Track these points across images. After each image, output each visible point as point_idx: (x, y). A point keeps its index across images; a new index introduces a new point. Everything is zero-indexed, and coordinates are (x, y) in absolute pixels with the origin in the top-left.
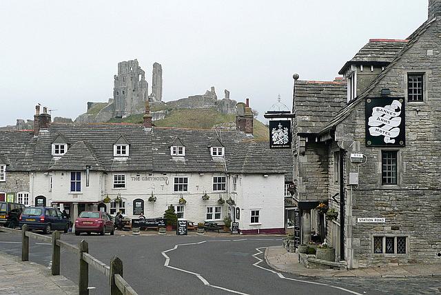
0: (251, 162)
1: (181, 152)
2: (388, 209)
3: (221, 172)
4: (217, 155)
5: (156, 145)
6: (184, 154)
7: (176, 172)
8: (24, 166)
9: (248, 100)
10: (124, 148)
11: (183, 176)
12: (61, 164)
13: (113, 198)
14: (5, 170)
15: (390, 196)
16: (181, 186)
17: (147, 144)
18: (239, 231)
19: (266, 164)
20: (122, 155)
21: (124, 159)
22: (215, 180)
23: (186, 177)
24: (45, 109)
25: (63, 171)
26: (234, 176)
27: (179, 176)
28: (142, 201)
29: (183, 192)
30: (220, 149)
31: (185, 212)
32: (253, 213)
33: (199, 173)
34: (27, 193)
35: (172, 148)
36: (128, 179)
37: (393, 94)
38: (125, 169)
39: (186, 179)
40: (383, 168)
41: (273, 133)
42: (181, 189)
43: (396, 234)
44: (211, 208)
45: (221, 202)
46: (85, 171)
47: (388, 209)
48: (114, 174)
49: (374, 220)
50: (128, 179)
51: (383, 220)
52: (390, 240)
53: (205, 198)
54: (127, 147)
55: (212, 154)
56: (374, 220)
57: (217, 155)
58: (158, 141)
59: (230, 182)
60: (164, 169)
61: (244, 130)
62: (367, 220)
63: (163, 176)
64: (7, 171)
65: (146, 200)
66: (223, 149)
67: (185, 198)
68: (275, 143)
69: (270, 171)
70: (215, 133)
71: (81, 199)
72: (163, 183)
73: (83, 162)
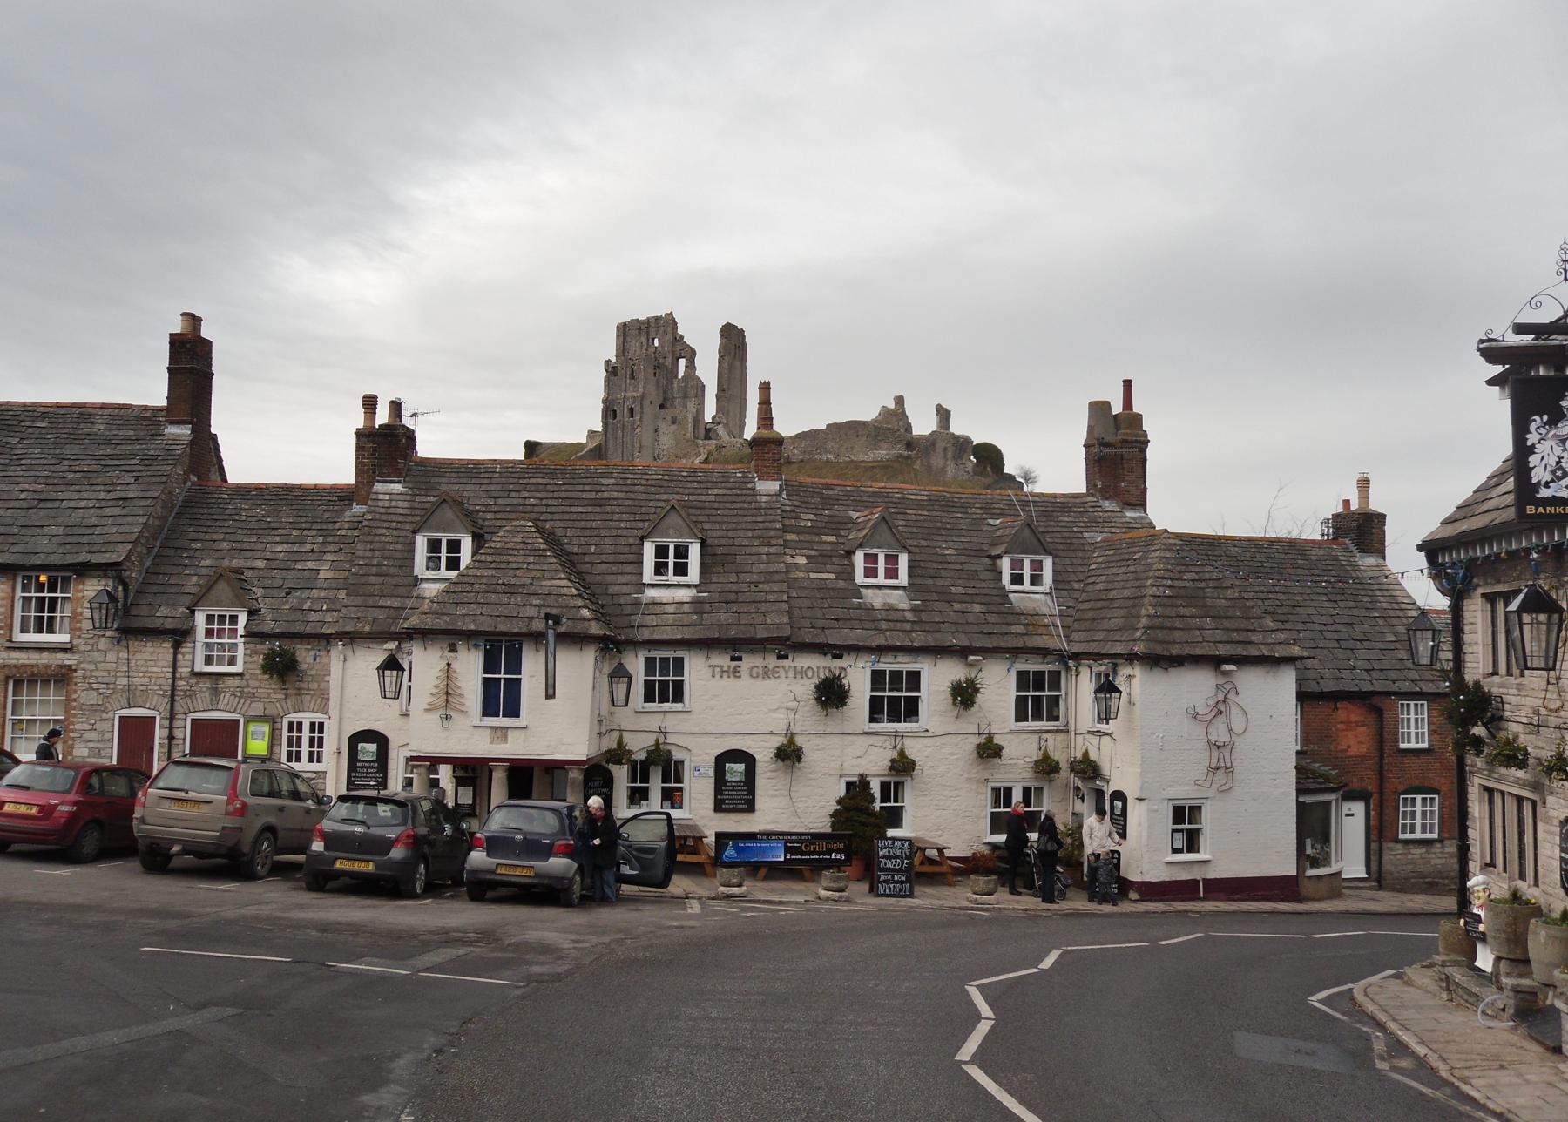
0: (1168, 612)
1: (892, 573)
3: (1043, 653)
4: (1027, 586)
5: (798, 546)
6: (903, 579)
7: (881, 650)
8: (313, 617)
9: (1128, 384)
10: (682, 552)
11: (904, 664)
13: (639, 745)
14: (241, 631)
16: (894, 701)
17: (766, 541)
18: (1125, 886)
19: (1227, 623)
20: (672, 578)
21: (685, 595)
23: (913, 667)
24: (396, 407)
27: (888, 664)
28: (747, 759)
29: (902, 726)
30: (1037, 566)
31: (910, 802)
32: (1179, 814)
34: (317, 717)
35: (859, 558)
36: (697, 671)
38: (687, 634)
39: (914, 679)
41: (1532, 438)
42: (895, 718)
44: (1008, 792)
45: (1046, 767)
46: (537, 638)
50: (697, 671)
53: (989, 751)
55: (1006, 579)
57: (1027, 586)
59: (1081, 690)
60: (835, 638)
64: (250, 634)
65: (763, 753)
66: (1048, 564)
67: (914, 750)
68: (1544, 493)
69: (1240, 650)
70: (1010, 504)
71: (518, 746)
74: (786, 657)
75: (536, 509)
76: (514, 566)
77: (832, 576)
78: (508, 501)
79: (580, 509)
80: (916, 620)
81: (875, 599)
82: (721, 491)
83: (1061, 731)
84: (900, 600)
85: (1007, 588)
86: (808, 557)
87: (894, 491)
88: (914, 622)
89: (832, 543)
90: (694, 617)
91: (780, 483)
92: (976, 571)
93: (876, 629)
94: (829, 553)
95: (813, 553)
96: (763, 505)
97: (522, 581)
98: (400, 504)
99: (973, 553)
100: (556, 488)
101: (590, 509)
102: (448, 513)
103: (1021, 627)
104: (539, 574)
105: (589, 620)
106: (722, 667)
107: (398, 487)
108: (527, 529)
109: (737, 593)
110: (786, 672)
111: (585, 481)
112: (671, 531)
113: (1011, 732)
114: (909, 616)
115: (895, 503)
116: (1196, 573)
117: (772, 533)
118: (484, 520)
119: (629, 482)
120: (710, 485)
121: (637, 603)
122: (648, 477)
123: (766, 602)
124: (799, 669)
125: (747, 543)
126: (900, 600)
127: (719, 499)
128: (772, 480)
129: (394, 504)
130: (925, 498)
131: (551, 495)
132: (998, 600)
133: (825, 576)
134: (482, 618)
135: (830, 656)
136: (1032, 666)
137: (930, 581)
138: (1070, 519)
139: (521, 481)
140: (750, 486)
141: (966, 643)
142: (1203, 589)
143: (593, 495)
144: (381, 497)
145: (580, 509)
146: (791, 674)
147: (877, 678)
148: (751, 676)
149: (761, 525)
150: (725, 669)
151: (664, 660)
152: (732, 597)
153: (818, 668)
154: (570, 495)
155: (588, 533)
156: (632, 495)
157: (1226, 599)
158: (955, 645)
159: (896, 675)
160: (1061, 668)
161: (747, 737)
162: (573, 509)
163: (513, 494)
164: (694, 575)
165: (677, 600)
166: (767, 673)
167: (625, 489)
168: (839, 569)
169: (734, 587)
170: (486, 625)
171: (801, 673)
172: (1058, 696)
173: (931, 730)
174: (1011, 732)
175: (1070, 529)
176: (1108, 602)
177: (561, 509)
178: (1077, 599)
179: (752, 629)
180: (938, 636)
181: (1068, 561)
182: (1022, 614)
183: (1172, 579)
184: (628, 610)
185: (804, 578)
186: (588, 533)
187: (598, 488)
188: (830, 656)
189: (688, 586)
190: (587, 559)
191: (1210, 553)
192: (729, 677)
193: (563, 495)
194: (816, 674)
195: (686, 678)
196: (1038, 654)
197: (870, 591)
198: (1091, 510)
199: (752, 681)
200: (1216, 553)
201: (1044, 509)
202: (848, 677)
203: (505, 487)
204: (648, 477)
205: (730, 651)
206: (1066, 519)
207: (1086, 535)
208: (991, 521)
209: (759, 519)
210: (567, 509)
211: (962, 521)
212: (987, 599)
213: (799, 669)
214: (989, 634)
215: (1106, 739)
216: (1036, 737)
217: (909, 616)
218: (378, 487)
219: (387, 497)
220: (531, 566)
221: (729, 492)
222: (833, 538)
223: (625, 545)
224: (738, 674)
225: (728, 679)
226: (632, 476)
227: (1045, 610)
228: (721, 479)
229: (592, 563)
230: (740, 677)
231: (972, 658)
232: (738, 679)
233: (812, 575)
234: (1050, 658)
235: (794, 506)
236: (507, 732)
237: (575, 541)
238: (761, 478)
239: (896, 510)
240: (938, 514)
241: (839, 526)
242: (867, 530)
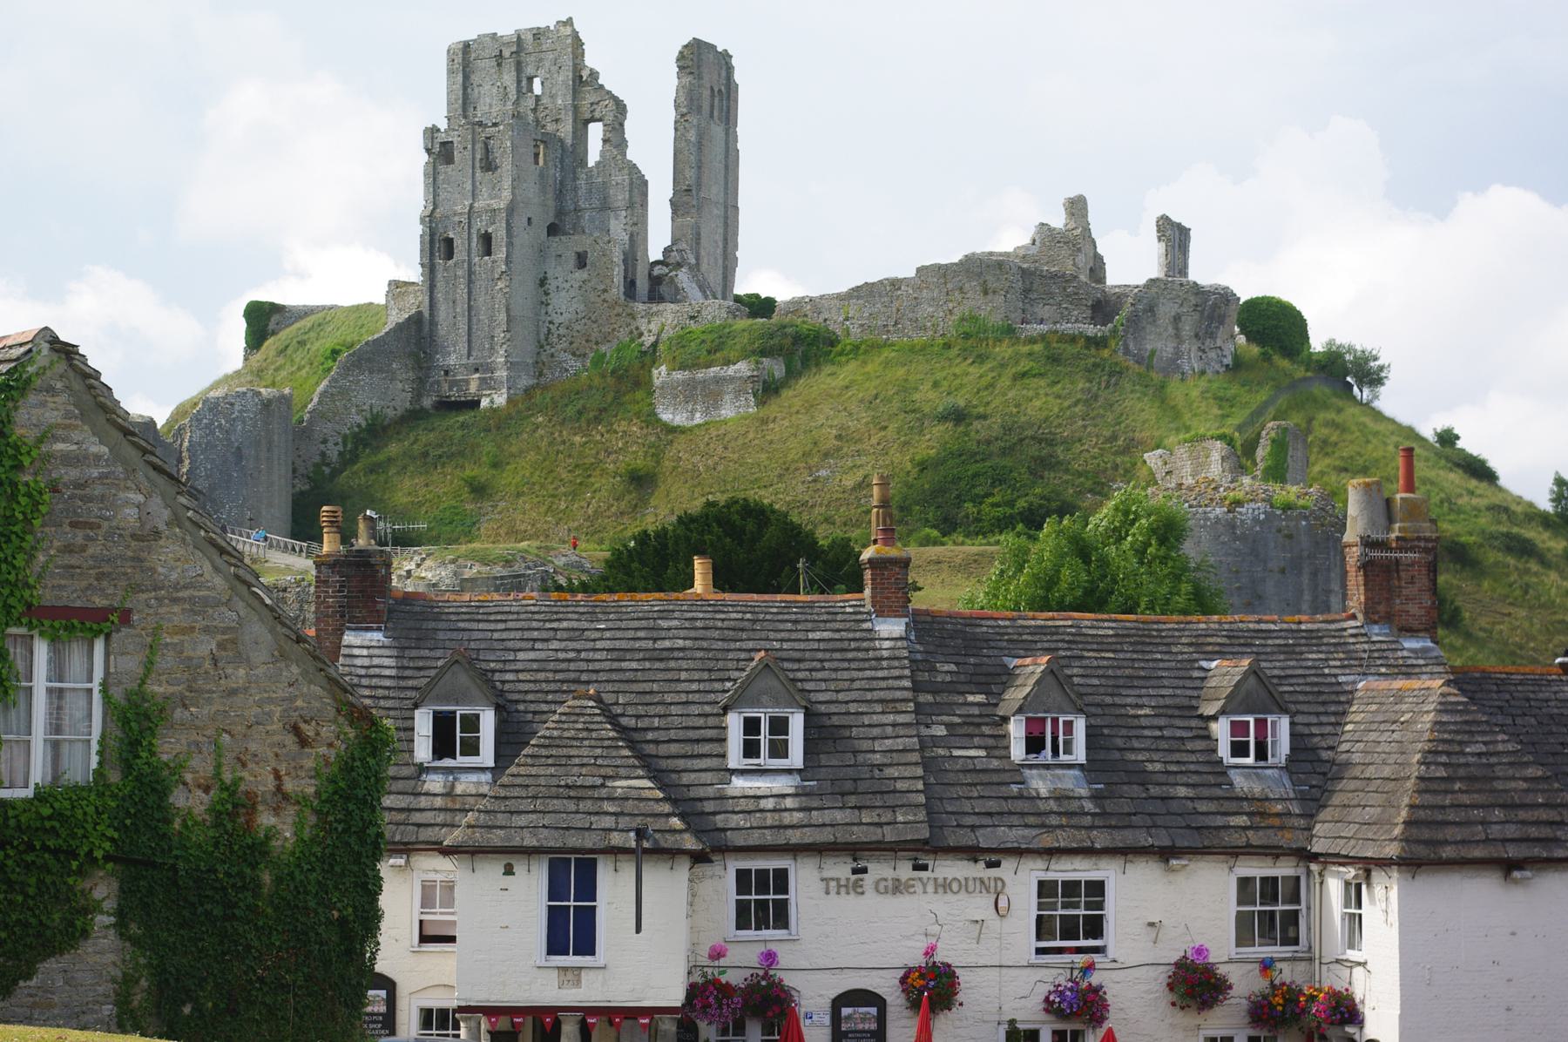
0: (1438, 800)
3: (1273, 853)
7: (1051, 853)
10: (780, 726)
11: (1080, 870)
12: (501, 819)
20: (764, 760)
23: (1094, 875)
25: (511, 854)
26: (1350, 872)
39: (1097, 888)
48: (734, 864)
54: (797, 723)
55: (1224, 751)
58: (951, 688)
60: (984, 839)
63: (978, 870)
72: (980, 906)
73: (609, 807)
74: (925, 868)
75: (572, 666)
76: (577, 761)
77: (982, 753)
78: (532, 655)
79: (634, 665)
80: (1097, 810)
82: (826, 635)
83: (1301, 959)
84: (1072, 782)
85: (1225, 761)
86: (948, 726)
87: (1066, 623)
88: (1094, 815)
89: (979, 704)
90: (800, 815)
93: (1043, 826)
95: (957, 720)
96: (885, 654)
97: (589, 781)
98: (387, 662)
99: (1177, 712)
100: (597, 635)
101: (647, 665)
102: (462, 678)
103: (1245, 818)
104: (610, 772)
105: (681, 831)
106: (838, 880)
107: (377, 637)
108: (589, 711)
109: (855, 780)
110: (924, 886)
111: (636, 624)
112: (765, 699)
114: (1089, 806)
116: (1485, 743)
117: (898, 694)
118: (503, 682)
119: (699, 624)
120: (810, 626)
121: (723, 798)
122: (723, 616)
124: (940, 881)
125: (865, 710)
126: (1072, 782)
127: (822, 645)
128: (895, 616)
129: (376, 661)
130: (1111, 632)
131: (590, 645)
132: (1212, 779)
133: (972, 753)
134: (546, 832)
135: (982, 865)
136: (1256, 869)
137: (1117, 755)
138: (1321, 656)
139: (548, 625)
140: (867, 625)
141: (1167, 843)
142: (1492, 765)
143: (650, 644)
144: (356, 652)
145: (634, 665)
146: (930, 888)
148: (878, 891)
149: (883, 684)
150: (843, 883)
151: (763, 874)
152: (849, 786)
153: (966, 879)
154: (617, 644)
155: (648, 698)
156: (705, 644)
157: (1525, 779)
158: (1152, 846)
159: (1071, 888)
160: (1301, 872)
161: (874, 973)
162: (624, 665)
163: (538, 645)
164: (796, 757)
165: (775, 792)
166: (898, 888)
167: (693, 634)
169: (851, 772)
170: (551, 839)
171: (944, 887)
172: (1296, 912)
173: (1120, 960)
175: (1319, 672)
176: (1365, 782)
177: (607, 665)
178: (1324, 774)
179: (879, 830)
180: (1128, 833)
181: (1314, 720)
182: (1246, 799)
183: (1448, 754)
184: (709, 807)
185: (944, 757)
186: (648, 698)
187: (655, 634)
188: (982, 865)
189: (789, 771)
190: (650, 736)
191: (1532, 696)
192: (848, 893)
193: (607, 644)
195: (792, 896)
196: (1266, 855)
197: (1034, 772)
198: (1352, 640)
199: (881, 898)
200: (1541, 696)
202: (1007, 890)
203: (527, 635)
204: (723, 616)
205: (850, 860)
206: (1314, 656)
207: (1342, 679)
208: (1204, 664)
209: (880, 674)
210: (615, 665)
211: (1161, 665)
212: (1194, 779)
213: (940, 881)
214: (1198, 828)
215: (1358, 971)
217: (1089, 806)
218: (349, 638)
219: (365, 652)
220: (599, 762)
221: (837, 636)
222: (980, 698)
223: (699, 715)
224: (859, 890)
225: (847, 897)
226: (701, 615)
228: (825, 617)
229: (656, 742)
230: (863, 893)
231: (1174, 862)
232: (861, 897)
233: (956, 753)
234: (1283, 861)
235: (927, 652)
236: (579, 975)
237: (630, 711)
239: (1069, 653)
240: (1128, 655)
241: (990, 679)
242: (1028, 689)
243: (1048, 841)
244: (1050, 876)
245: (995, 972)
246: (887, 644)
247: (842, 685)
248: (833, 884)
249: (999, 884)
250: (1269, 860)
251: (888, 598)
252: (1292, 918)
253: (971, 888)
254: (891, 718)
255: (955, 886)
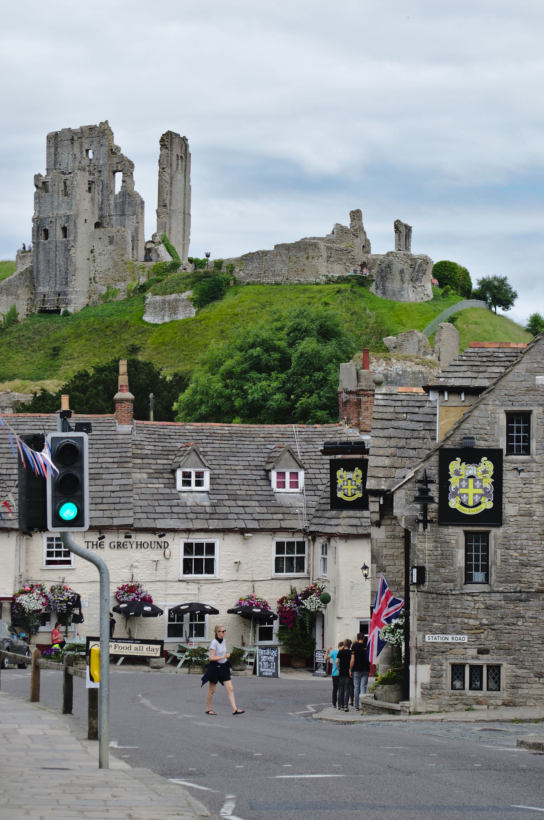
1: (199, 483)
2: (472, 622)
4: (288, 489)
6: (206, 486)
7: (188, 531)
15: (476, 602)
16: (198, 562)
22: (280, 547)
33: (242, 531)
37: (481, 444)
39: (211, 548)
40: (468, 558)
42: (199, 571)
43: (484, 660)
47: (472, 622)
49: (450, 638)
51: (465, 638)
52: (476, 670)
56: (450, 638)
57: (288, 489)
60: (161, 524)
61: (358, 425)
62: (439, 638)
63: (154, 538)
66: (302, 474)
72: (156, 554)
74: (130, 537)
77: (163, 486)
81: (189, 499)
83: (305, 578)
91: (132, 426)
92: (255, 480)
94: (162, 471)
95: (151, 471)
103: (281, 515)
109: (102, 498)
113: (273, 579)
114: (208, 510)
115: (207, 436)
123: (119, 503)
124: (139, 543)
135: (157, 536)
137: (224, 487)
141: (244, 526)
146: (134, 546)
147: (188, 548)
159: (199, 546)
166: (120, 546)
168: (167, 481)
172: (304, 557)
174: (273, 579)
181: (318, 471)
188: (157, 536)
194: (149, 546)
197: (185, 494)
201: (306, 436)
205: (98, 533)
213: (139, 543)
214: (258, 520)
216: (250, 584)
224: (102, 547)
225: (97, 550)
227: (297, 504)
231: (246, 535)
232: (103, 550)
238: (120, 423)
243: (189, 525)
244: (190, 541)
245: (162, 584)
246: (121, 437)
247: (101, 455)
248: (90, 544)
249: (166, 544)
250: (290, 535)
251: (123, 416)
252: (301, 561)
253: (153, 546)
254: (121, 470)
255: (146, 545)
